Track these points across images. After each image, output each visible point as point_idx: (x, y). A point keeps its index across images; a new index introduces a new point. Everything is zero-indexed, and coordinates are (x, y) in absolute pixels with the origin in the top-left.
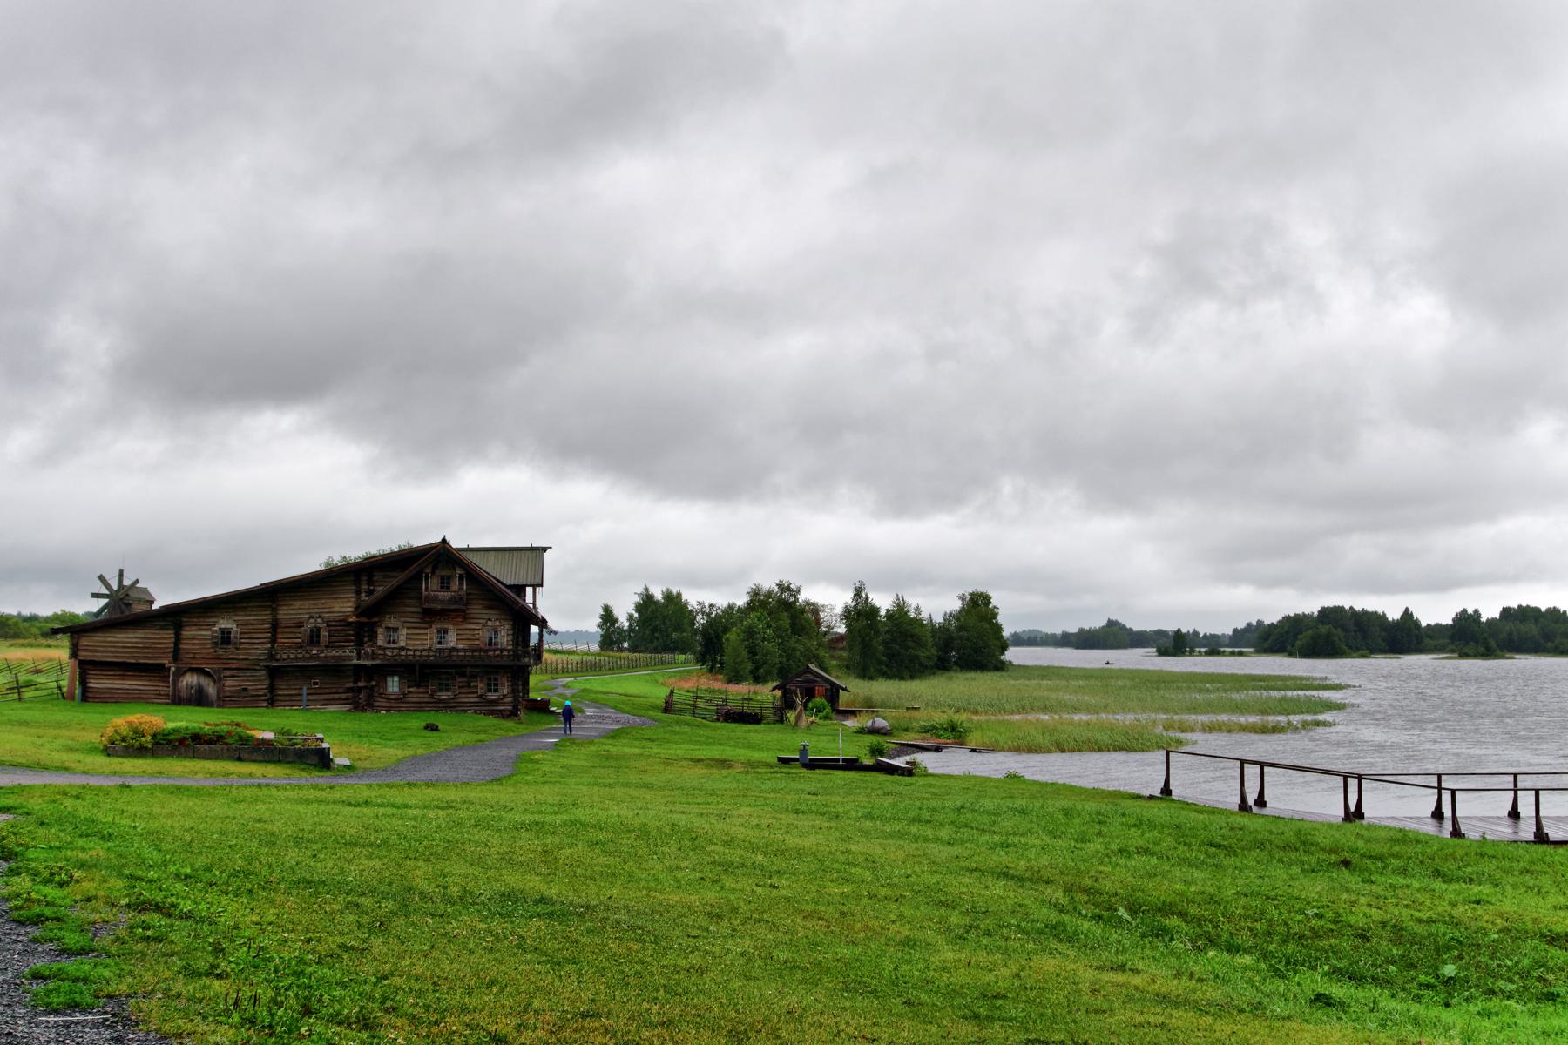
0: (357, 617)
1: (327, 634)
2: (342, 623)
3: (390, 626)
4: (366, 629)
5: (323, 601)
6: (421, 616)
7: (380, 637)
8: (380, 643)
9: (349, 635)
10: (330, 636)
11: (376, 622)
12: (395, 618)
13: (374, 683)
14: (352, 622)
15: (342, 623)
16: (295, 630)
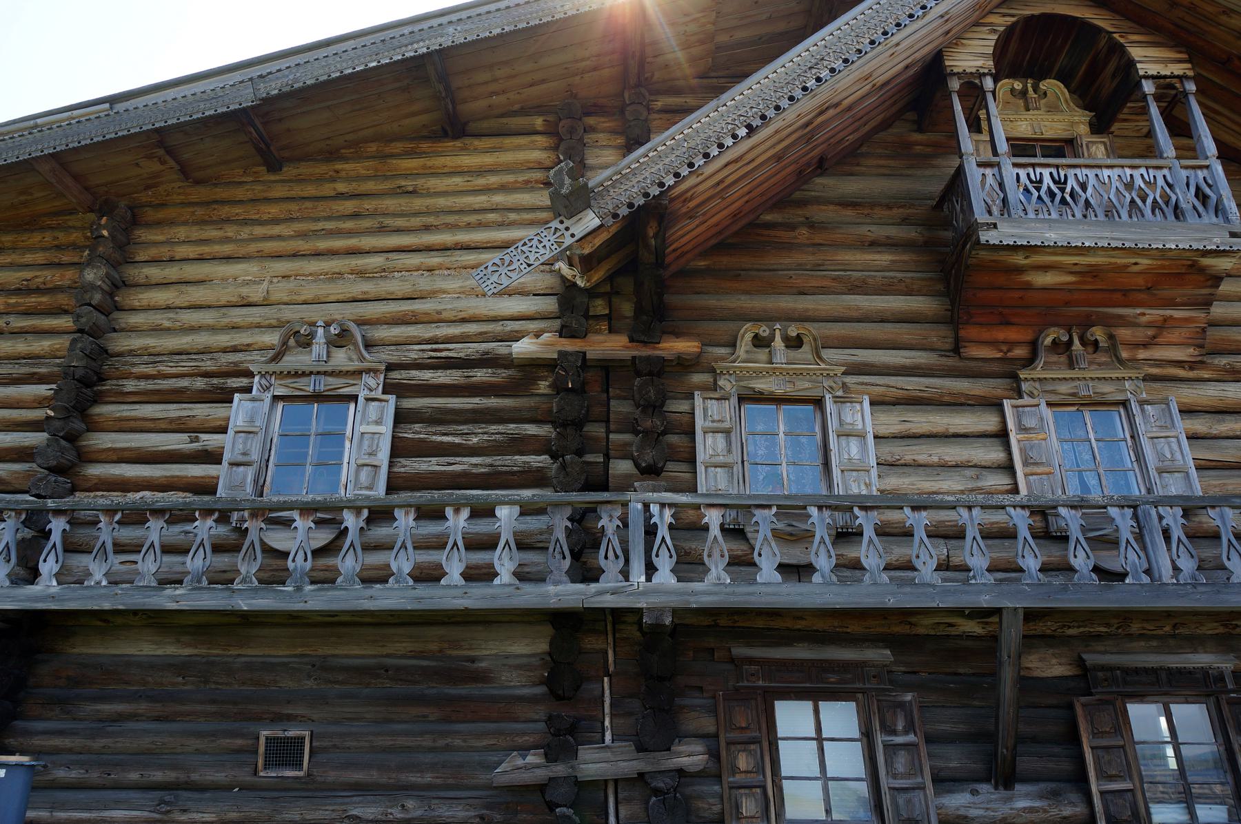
0: (565, 332)
1: (386, 429)
2: (481, 375)
3: (761, 385)
4: (621, 408)
5: (376, 261)
6: (938, 335)
7: (708, 447)
8: (711, 480)
9: (518, 445)
10: (399, 449)
11: (685, 365)
12: (794, 343)
13: (690, 756)
14: (531, 368)
15: (481, 375)
16: (201, 411)
